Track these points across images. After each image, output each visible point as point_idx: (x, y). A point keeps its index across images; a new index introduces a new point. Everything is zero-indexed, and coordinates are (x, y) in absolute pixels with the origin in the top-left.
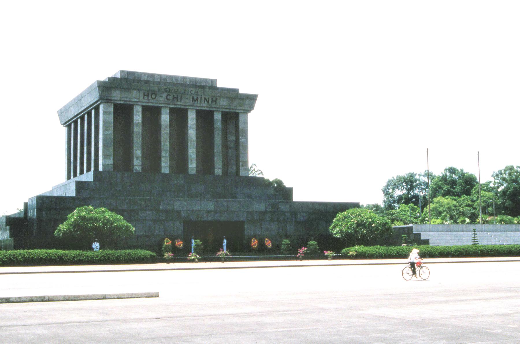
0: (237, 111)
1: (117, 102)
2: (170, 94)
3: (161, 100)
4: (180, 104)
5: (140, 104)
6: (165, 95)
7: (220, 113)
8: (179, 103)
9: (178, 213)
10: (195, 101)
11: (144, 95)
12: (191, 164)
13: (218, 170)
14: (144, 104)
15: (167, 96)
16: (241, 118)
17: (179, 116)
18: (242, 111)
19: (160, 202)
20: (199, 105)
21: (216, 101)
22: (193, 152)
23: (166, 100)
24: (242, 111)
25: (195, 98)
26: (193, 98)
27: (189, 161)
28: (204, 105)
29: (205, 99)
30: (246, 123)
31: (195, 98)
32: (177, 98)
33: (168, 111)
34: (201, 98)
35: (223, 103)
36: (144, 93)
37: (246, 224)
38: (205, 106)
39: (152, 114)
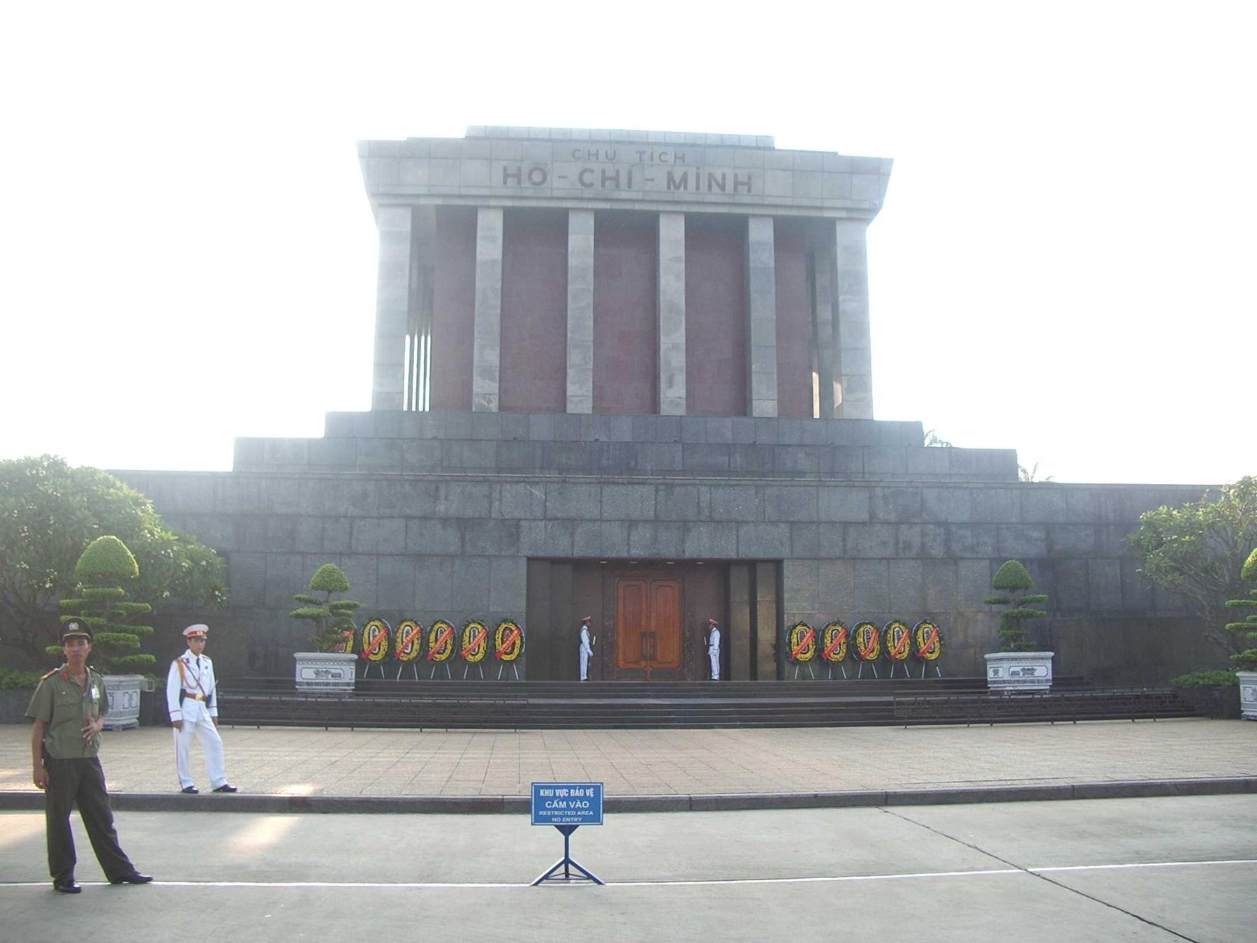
0: (827, 214)
1: (422, 201)
2: (588, 166)
3: (560, 186)
4: (629, 198)
5: (493, 203)
6: (573, 170)
7: (770, 223)
8: (624, 195)
9: (512, 530)
10: (677, 187)
11: (506, 176)
12: (670, 384)
13: (765, 403)
14: (509, 203)
15: (581, 174)
16: (843, 234)
17: (628, 234)
18: (843, 214)
19: (437, 488)
20: (689, 198)
21: (748, 184)
22: (675, 347)
23: (579, 185)
24: (843, 214)
25: (677, 177)
26: (670, 179)
27: (663, 377)
28: (708, 198)
29: (711, 175)
30: (858, 253)
31: (677, 177)
32: (616, 179)
33: (592, 223)
34: (698, 175)
35: (775, 189)
36: (505, 169)
37: (788, 569)
38: (714, 203)
39: (535, 231)
